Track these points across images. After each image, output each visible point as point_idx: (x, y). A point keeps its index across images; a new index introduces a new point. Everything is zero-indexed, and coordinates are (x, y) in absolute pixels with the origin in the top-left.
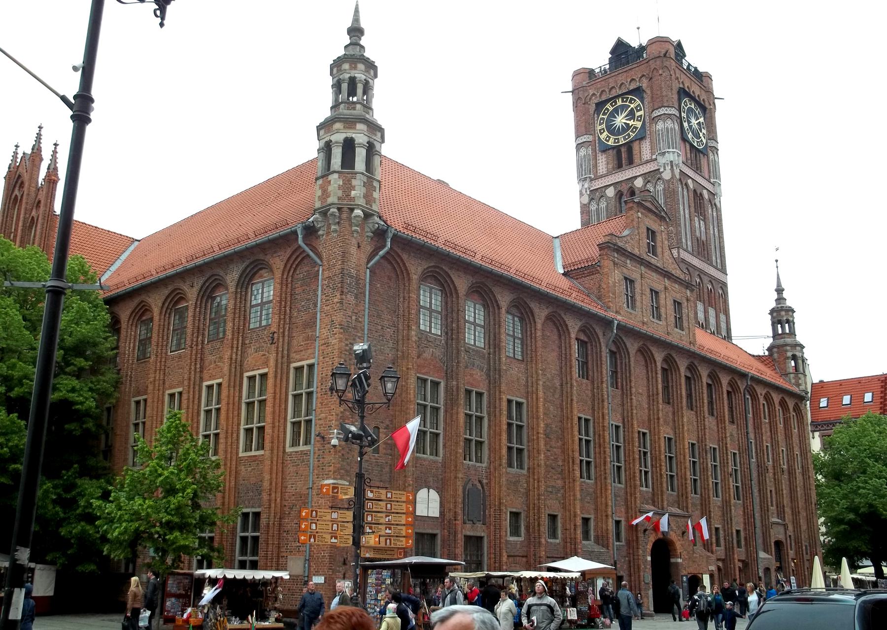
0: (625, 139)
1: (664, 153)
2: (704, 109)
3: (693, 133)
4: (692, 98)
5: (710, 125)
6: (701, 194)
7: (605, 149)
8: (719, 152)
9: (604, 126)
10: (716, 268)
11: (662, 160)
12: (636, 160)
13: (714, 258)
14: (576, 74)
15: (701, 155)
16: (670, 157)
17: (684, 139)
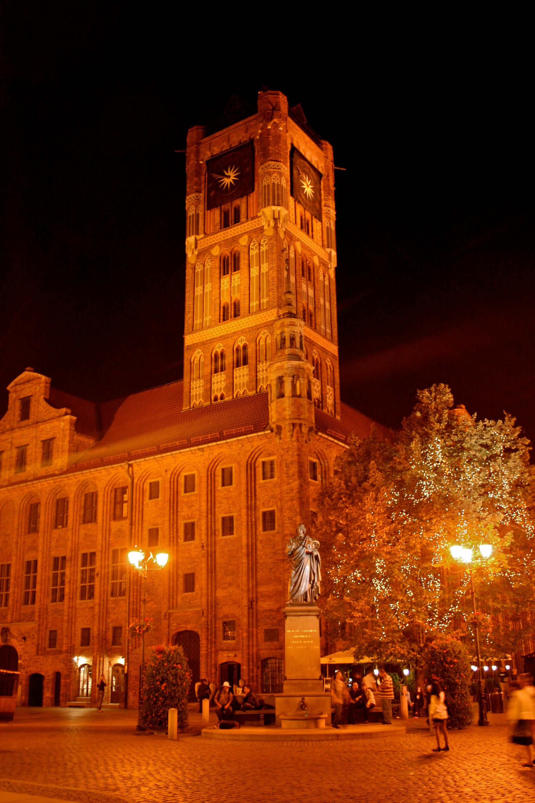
10: (325, 337)
12: (243, 219)
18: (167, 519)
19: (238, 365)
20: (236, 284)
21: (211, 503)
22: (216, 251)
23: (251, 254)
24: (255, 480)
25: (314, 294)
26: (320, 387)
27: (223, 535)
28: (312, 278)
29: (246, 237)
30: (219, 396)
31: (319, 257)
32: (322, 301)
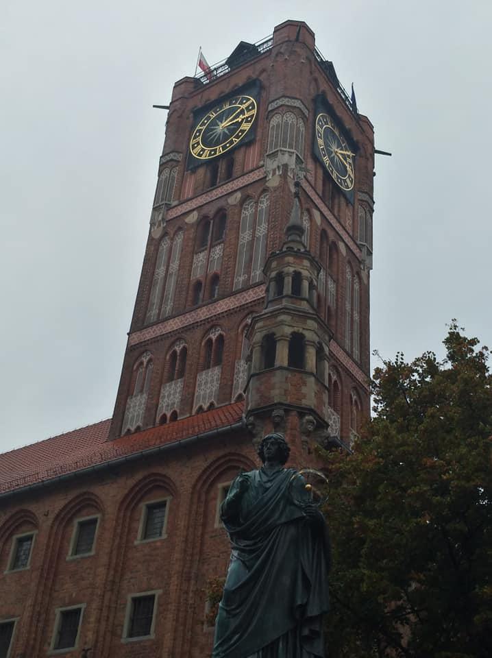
0: (224, 148)
1: (274, 155)
2: (354, 146)
3: (332, 160)
4: (337, 122)
5: (366, 177)
6: (334, 247)
7: (192, 165)
8: (374, 214)
9: (199, 139)
10: (350, 355)
11: (271, 165)
12: (235, 175)
13: (348, 342)
14: (177, 85)
15: (342, 199)
16: (285, 159)
17: (317, 160)
18: (29, 602)
19: (207, 367)
20: (216, 257)
21: (116, 571)
22: (193, 218)
23: (243, 216)
24: (204, 525)
25: (337, 290)
26: (339, 425)
27: (130, 635)
28: (335, 269)
29: (239, 195)
30: (169, 415)
31: (346, 245)
32: (348, 307)
